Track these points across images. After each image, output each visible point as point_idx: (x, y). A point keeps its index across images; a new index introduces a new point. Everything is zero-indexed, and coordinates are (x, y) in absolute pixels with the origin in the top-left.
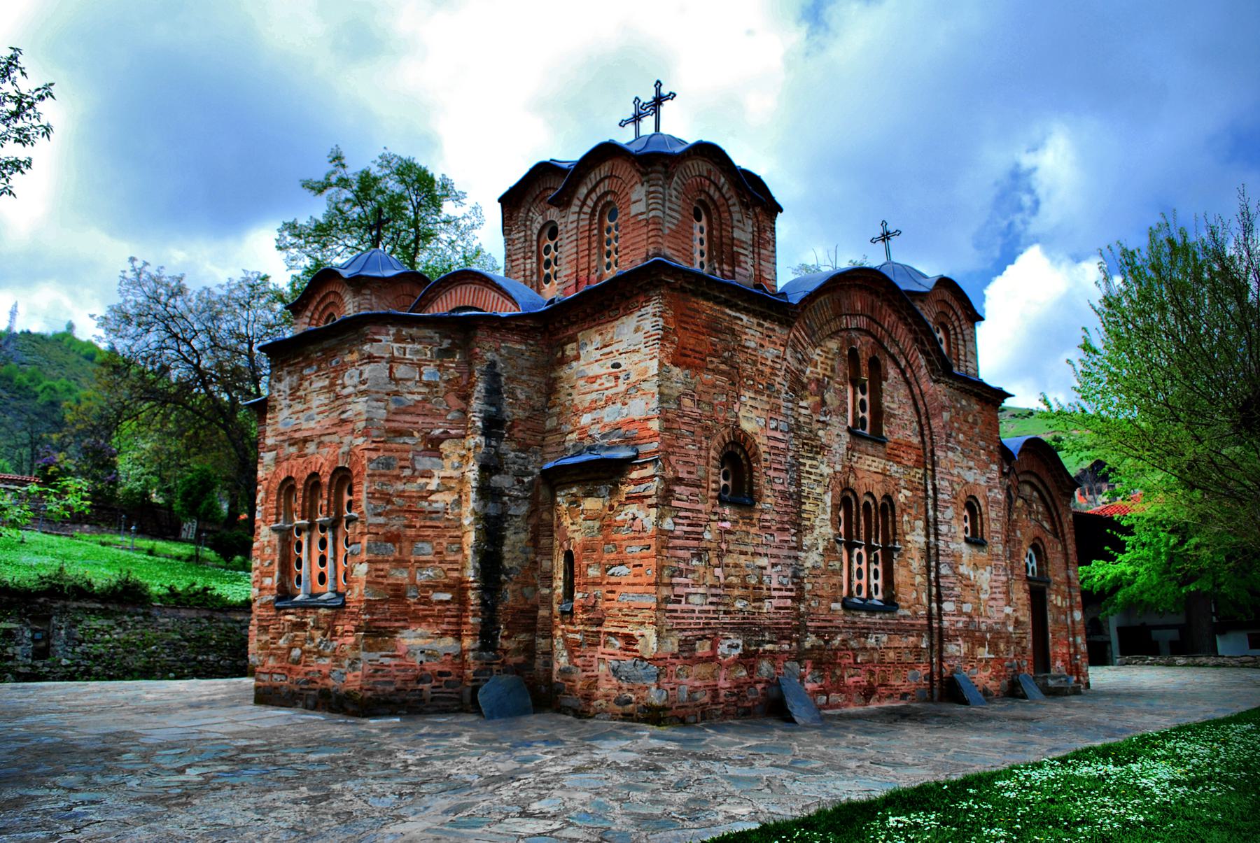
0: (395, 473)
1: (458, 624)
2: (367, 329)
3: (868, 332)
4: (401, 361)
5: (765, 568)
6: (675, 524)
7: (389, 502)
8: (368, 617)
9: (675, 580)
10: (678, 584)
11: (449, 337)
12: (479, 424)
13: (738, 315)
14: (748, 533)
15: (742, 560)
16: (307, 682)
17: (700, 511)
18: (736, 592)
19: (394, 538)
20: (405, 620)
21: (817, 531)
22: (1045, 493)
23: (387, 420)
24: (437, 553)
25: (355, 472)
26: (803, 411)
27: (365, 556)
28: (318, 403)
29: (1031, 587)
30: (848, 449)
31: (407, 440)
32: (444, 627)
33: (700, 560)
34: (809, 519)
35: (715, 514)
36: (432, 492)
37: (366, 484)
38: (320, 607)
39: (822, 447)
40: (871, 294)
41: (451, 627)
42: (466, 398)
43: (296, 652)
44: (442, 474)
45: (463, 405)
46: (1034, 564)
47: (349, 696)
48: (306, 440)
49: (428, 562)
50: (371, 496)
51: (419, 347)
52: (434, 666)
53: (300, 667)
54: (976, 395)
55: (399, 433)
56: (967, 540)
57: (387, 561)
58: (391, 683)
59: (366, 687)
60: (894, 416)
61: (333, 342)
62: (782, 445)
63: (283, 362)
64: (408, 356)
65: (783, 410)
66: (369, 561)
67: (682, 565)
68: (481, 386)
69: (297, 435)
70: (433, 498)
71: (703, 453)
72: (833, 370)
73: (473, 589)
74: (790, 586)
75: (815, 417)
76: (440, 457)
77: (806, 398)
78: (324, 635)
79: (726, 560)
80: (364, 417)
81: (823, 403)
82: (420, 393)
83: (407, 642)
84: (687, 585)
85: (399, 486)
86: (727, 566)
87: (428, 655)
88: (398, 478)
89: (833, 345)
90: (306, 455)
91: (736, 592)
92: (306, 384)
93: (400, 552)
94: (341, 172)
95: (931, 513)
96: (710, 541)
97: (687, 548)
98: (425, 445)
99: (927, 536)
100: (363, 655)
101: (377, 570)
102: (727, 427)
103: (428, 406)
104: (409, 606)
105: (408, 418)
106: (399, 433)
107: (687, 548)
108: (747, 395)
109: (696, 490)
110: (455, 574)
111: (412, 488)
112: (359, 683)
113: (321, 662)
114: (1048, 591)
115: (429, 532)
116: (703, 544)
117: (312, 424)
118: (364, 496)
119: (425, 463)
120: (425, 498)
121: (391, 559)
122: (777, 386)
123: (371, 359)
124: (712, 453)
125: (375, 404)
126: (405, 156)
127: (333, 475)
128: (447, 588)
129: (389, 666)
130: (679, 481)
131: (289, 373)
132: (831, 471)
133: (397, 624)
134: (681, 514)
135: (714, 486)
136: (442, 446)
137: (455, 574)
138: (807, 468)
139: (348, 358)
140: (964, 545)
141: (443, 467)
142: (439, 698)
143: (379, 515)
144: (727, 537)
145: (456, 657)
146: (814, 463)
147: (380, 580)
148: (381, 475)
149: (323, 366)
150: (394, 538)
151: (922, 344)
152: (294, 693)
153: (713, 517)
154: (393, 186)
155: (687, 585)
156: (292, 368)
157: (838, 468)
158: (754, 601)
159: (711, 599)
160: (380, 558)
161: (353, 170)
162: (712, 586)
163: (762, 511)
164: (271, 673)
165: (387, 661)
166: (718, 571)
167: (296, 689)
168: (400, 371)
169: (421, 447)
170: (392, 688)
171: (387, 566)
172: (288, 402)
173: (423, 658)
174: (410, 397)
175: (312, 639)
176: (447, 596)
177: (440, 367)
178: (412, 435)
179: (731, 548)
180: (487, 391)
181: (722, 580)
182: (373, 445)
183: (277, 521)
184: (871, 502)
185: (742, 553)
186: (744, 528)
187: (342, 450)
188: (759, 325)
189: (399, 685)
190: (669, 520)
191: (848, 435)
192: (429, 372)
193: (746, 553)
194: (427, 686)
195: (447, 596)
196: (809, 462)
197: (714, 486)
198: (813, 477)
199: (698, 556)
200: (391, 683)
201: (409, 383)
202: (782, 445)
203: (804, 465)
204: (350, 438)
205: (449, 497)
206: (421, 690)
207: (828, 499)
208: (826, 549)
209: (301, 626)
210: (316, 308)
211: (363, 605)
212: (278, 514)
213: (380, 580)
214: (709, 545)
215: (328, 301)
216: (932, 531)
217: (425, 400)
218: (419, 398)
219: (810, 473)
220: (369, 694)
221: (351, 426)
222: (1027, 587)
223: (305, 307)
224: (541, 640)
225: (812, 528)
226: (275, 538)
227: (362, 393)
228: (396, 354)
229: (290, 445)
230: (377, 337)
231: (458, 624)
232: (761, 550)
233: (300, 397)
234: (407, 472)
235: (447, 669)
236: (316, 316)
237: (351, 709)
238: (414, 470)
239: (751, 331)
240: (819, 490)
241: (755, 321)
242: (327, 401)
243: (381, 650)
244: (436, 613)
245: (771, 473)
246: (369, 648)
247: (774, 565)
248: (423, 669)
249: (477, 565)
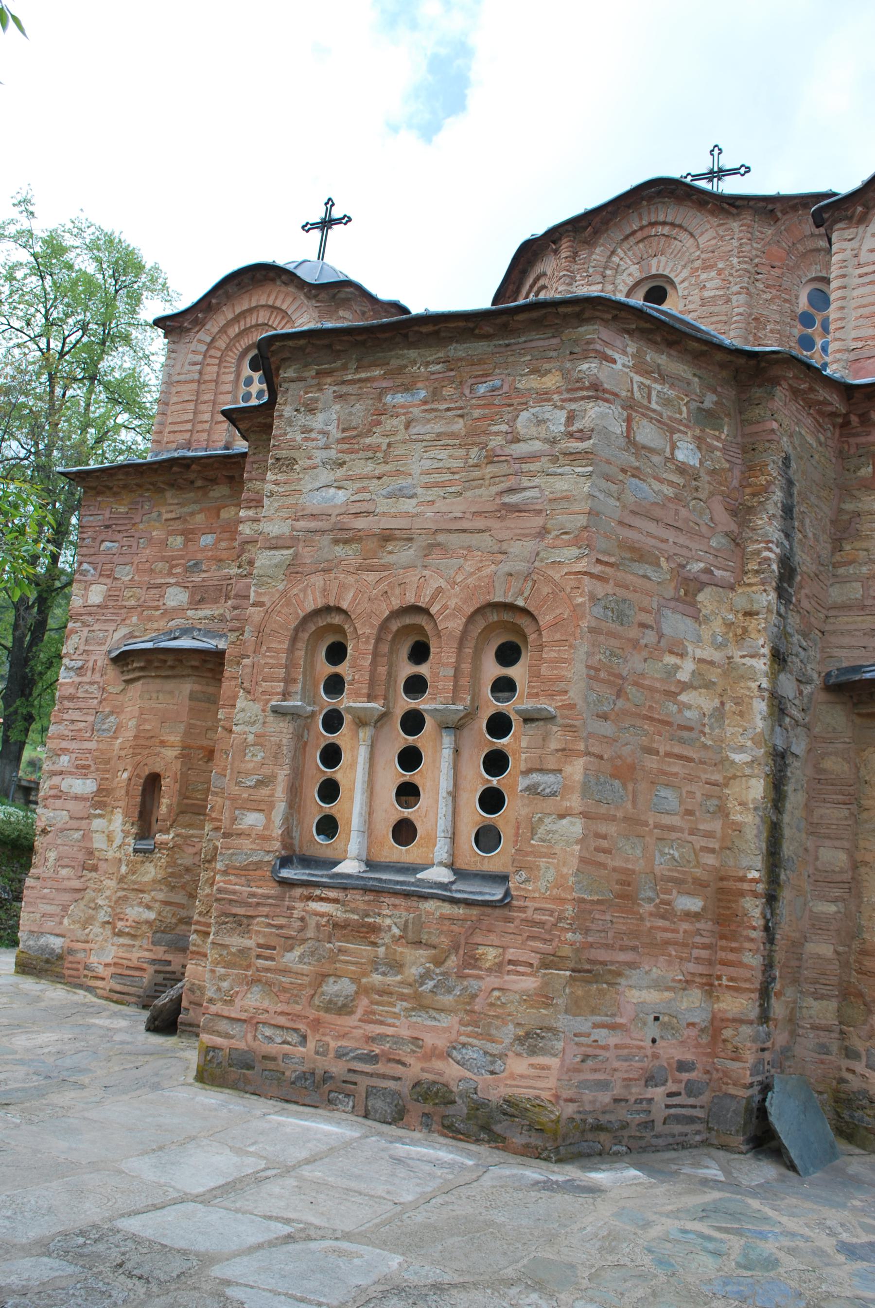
0: (633, 633)
1: (710, 963)
2: (595, 333)
4: (646, 412)
7: (620, 693)
8: (578, 937)
11: (715, 391)
12: (775, 567)
16: (373, 1058)
19: (625, 773)
20: (634, 949)
23: (621, 523)
24: (689, 813)
25: (545, 620)
27: (575, 802)
28: (427, 464)
31: (649, 571)
32: (691, 967)
36: (685, 687)
37: (583, 648)
38: (425, 897)
41: (701, 969)
42: (742, 513)
43: (339, 988)
44: (699, 653)
45: (733, 527)
47: (512, 1109)
48: (386, 537)
49: (672, 829)
50: (594, 673)
51: (671, 393)
52: (672, 1051)
53: (351, 1021)
55: (640, 555)
57: (613, 819)
58: (604, 1085)
59: (566, 1094)
61: (480, 348)
63: (329, 373)
64: (654, 406)
66: (585, 815)
69: (360, 523)
70: (683, 698)
73: (755, 894)
78: (439, 963)
80: (585, 507)
82: (671, 483)
83: (635, 996)
85: (636, 663)
87: (665, 1026)
88: (635, 644)
90: (386, 567)
92: (390, 423)
93: (634, 802)
94: (25, 223)
98: (677, 589)
100: (563, 1022)
101: (598, 836)
103: (683, 512)
104: (642, 919)
105: (652, 527)
106: (640, 555)
110: (710, 860)
112: (552, 1083)
113: (421, 1019)
115: (677, 767)
117: (408, 505)
119: (675, 624)
121: (620, 814)
123: (597, 391)
125: (604, 484)
126: (108, 229)
127: (471, 619)
128: (699, 886)
129: (605, 1048)
131: (339, 397)
133: (622, 957)
136: (700, 597)
137: (710, 860)
139: (533, 382)
141: (699, 639)
142: (678, 1119)
143: (605, 717)
145: (702, 1030)
147: (602, 857)
148: (611, 634)
149: (447, 391)
150: (625, 773)
152: (327, 1077)
154: (85, 264)
156: (345, 389)
160: (603, 810)
161: (41, 227)
164: (252, 1022)
165: (601, 1034)
167: (338, 1068)
168: (647, 433)
169: (670, 593)
170: (605, 1098)
171: (611, 829)
172: (333, 454)
173: (653, 1030)
174: (656, 485)
175: (396, 965)
176: (694, 904)
177: (700, 442)
178: (659, 565)
182: (597, 569)
183: (285, 695)
187: (505, 568)
189: (618, 1091)
192: (686, 453)
194: (658, 1093)
195: (694, 904)
200: (604, 1085)
201: (656, 459)
204: (530, 545)
205: (699, 702)
206: (650, 1100)
209: (367, 932)
210: (223, 330)
211: (569, 910)
212: (289, 680)
213: (602, 857)
215: (251, 320)
217: (677, 498)
218: (669, 491)
220: (570, 1109)
221: (539, 521)
223: (199, 324)
224: (811, 1001)
226: (282, 732)
227: (573, 456)
228: (637, 395)
229: (336, 542)
230: (609, 352)
231: (710, 963)
233: (375, 448)
234: (650, 637)
235: (689, 1057)
236: (221, 343)
237: (518, 1140)
238: (661, 636)
242: (456, 464)
243: (593, 1011)
244: (680, 936)
246: (575, 1008)
248: (656, 1056)
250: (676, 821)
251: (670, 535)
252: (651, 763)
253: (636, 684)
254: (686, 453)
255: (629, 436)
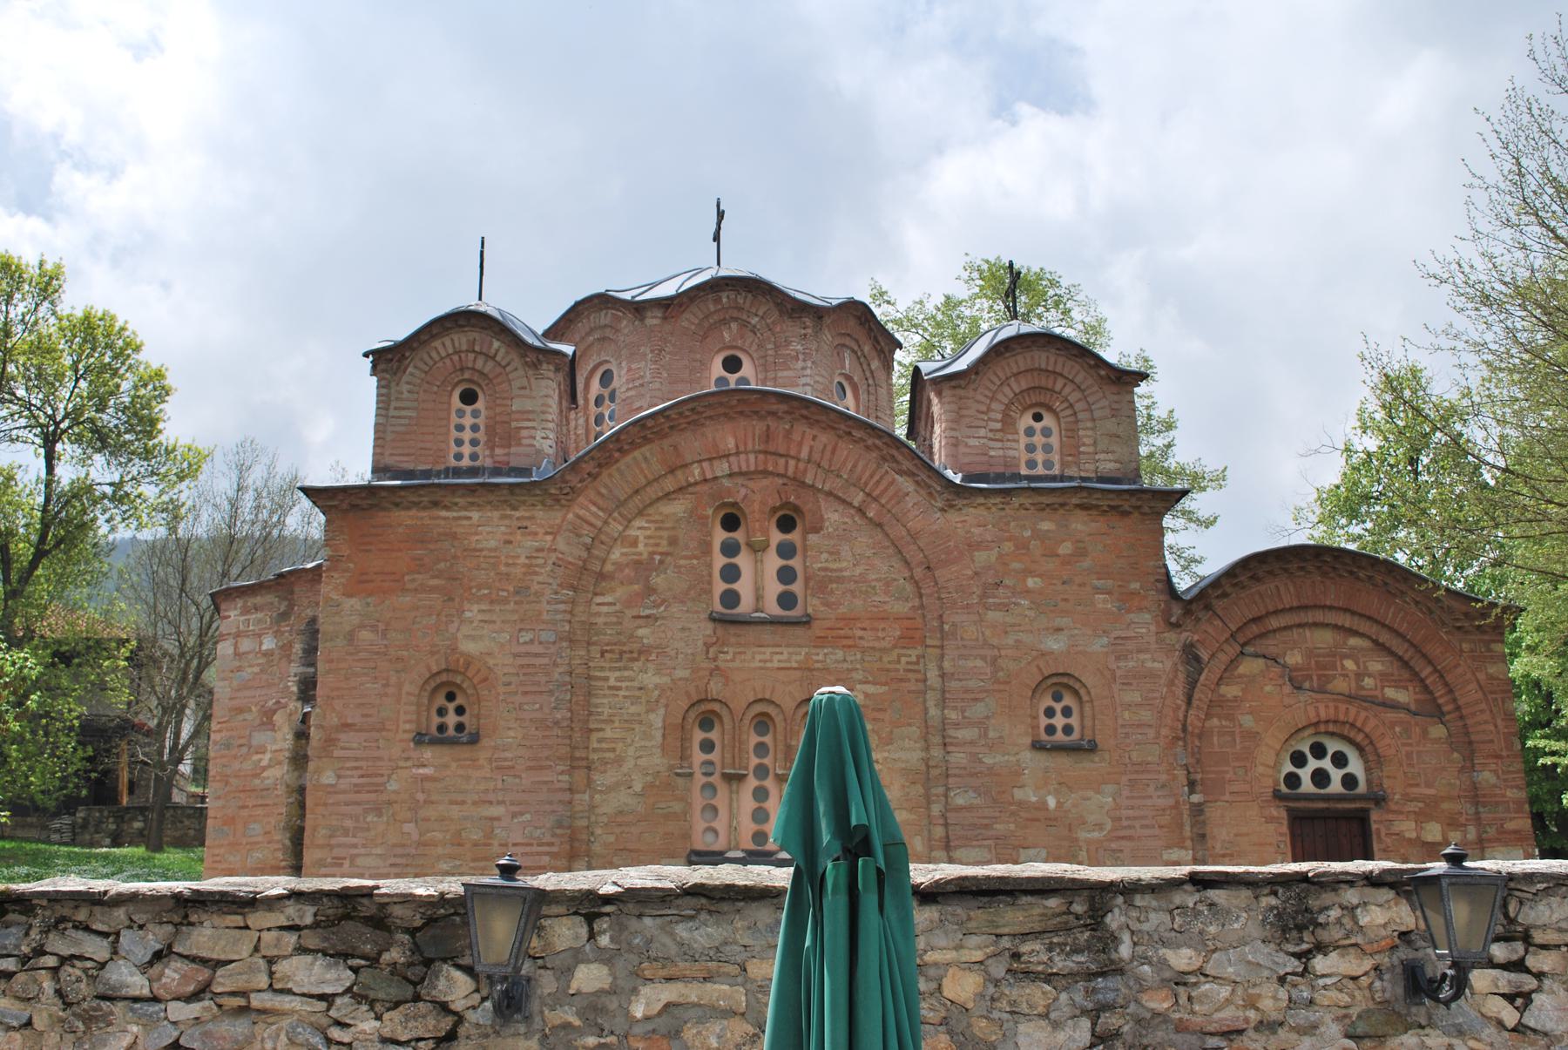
3: (765, 473)
5: (498, 819)
6: (339, 777)
7: (227, 783)
9: (333, 841)
10: (339, 846)
12: (295, 689)
13: (463, 513)
14: (468, 778)
15: (455, 812)
17: (380, 759)
18: (440, 850)
21: (630, 763)
22: (1384, 637)
26: (605, 609)
29: (1289, 810)
30: (708, 646)
33: (380, 815)
34: (614, 750)
35: (407, 759)
36: (264, 769)
39: (644, 651)
40: (762, 418)
44: (275, 747)
46: (1355, 766)
54: (1082, 507)
56: (1037, 746)
60: (840, 580)
62: (546, 661)
65: (545, 617)
67: (349, 823)
68: (298, 648)
71: (391, 690)
72: (673, 542)
74: (548, 838)
75: (630, 613)
76: (273, 730)
77: (613, 590)
79: (422, 813)
81: (650, 590)
84: (355, 846)
85: (236, 765)
86: (426, 820)
88: (235, 757)
89: (678, 508)
91: (440, 850)
95: (933, 711)
96: (394, 792)
97: (358, 803)
99: (927, 749)
102: (433, 653)
103: (264, 677)
105: (247, 693)
107: (358, 803)
108: (473, 612)
109: (375, 735)
111: (248, 765)
114: (1375, 816)
115: (260, 811)
116: (384, 797)
118: (1265, 755)
119: (259, 738)
120: (256, 776)
122: (535, 587)
124: (407, 688)
130: (346, 726)
132: (666, 680)
134: (349, 764)
135: (407, 726)
138: (612, 682)
140: (1027, 756)
144: (427, 785)
146: (626, 673)
151: (897, 462)
153: (402, 764)
155: (355, 846)
157: (680, 673)
158: (474, 860)
159: (393, 860)
162: (394, 846)
163: (495, 748)
166: (408, 827)
169: (258, 722)
171: (222, 851)
179: (434, 798)
180: (305, 651)
181: (415, 836)
184: (771, 710)
185: (452, 803)
186: (461, 772)
188: (510, 517)
190: (330, 773)
191: (710, 625)
193: (463, 803)
196: (618, 674)
197: (407, 726)
198: (622, 693)
199: (378, 811)
202: (546, 661)
203: (606, 679)
207: (657, 719)
208: (649, 787)
214: (393, 797)
216: (937, 740)
218: (256, 669)
219: (619, 688)
222: (1284, 814)
225: (619, 761)
232: (491, 797)
234: (244, 750)
239: (486, 528)
240: (633, 709)
241: (496, 514)
245: (519, 699)
247: (514, 815)
249: (288, 842)
250: (260, 839)
251: (258, 692)
252: (245, 813)
253: (236, 776)
254: (268, 643)
255: (237, 654)
